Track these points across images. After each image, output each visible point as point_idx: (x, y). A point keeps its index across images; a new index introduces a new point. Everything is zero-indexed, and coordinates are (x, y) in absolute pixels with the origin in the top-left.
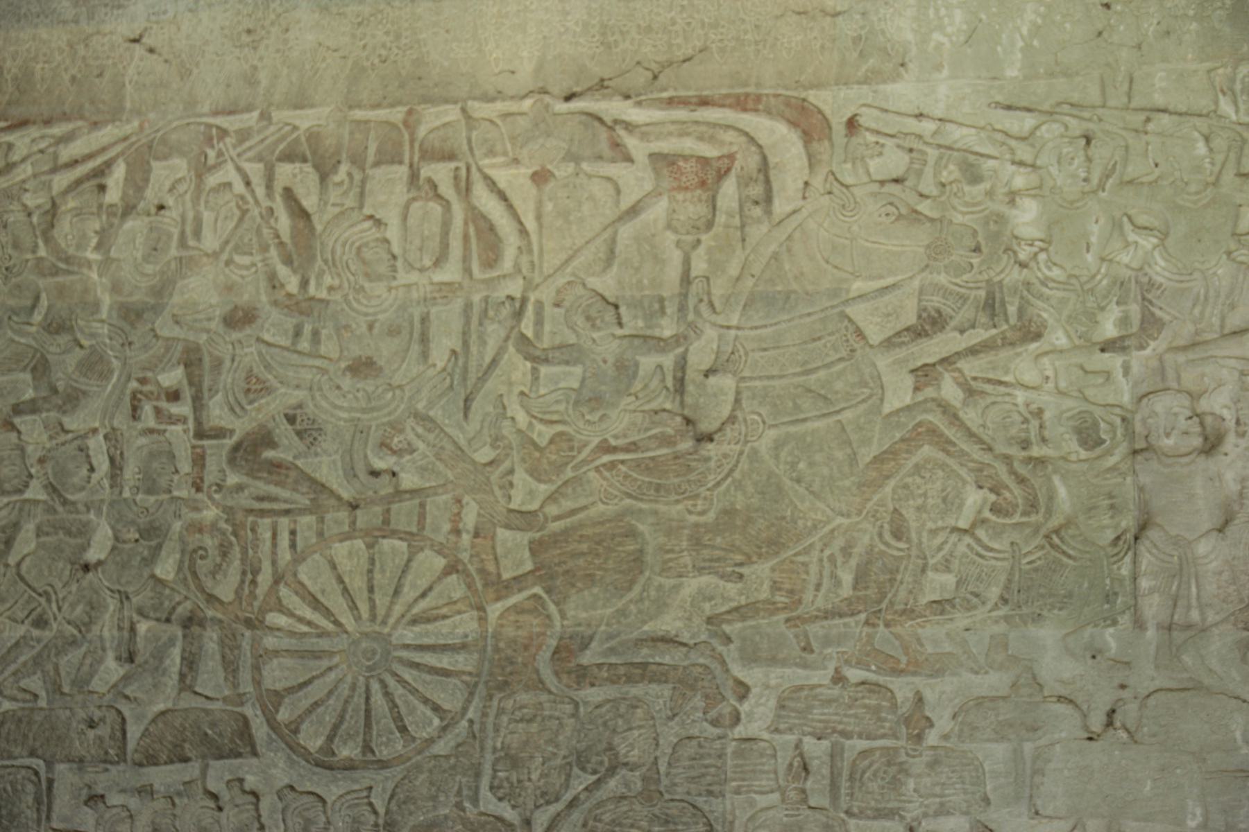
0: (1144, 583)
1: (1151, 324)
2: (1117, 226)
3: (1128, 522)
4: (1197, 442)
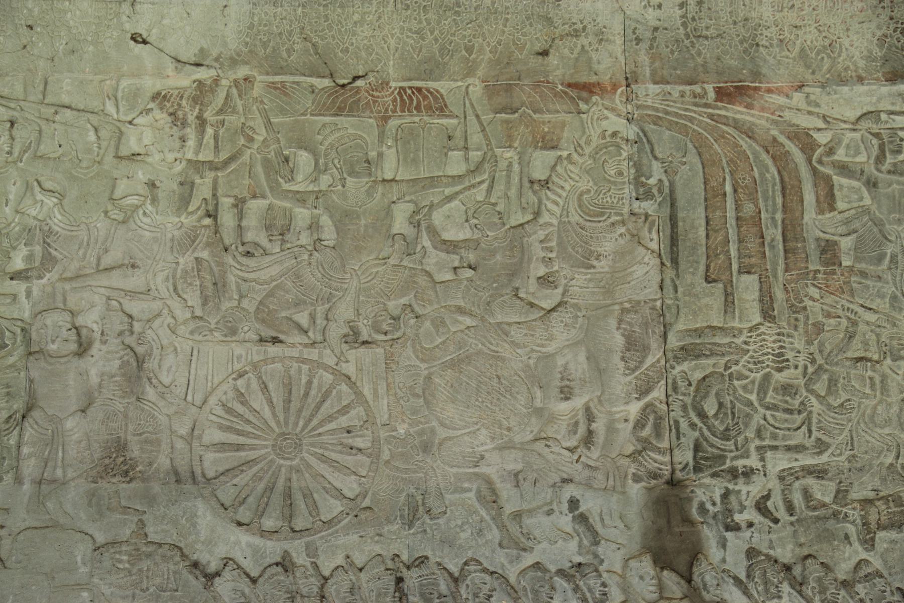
0: (25, 450)
1: (49, 261)
2: (28, 187)
3: (18, 405)
4: (73, 347)
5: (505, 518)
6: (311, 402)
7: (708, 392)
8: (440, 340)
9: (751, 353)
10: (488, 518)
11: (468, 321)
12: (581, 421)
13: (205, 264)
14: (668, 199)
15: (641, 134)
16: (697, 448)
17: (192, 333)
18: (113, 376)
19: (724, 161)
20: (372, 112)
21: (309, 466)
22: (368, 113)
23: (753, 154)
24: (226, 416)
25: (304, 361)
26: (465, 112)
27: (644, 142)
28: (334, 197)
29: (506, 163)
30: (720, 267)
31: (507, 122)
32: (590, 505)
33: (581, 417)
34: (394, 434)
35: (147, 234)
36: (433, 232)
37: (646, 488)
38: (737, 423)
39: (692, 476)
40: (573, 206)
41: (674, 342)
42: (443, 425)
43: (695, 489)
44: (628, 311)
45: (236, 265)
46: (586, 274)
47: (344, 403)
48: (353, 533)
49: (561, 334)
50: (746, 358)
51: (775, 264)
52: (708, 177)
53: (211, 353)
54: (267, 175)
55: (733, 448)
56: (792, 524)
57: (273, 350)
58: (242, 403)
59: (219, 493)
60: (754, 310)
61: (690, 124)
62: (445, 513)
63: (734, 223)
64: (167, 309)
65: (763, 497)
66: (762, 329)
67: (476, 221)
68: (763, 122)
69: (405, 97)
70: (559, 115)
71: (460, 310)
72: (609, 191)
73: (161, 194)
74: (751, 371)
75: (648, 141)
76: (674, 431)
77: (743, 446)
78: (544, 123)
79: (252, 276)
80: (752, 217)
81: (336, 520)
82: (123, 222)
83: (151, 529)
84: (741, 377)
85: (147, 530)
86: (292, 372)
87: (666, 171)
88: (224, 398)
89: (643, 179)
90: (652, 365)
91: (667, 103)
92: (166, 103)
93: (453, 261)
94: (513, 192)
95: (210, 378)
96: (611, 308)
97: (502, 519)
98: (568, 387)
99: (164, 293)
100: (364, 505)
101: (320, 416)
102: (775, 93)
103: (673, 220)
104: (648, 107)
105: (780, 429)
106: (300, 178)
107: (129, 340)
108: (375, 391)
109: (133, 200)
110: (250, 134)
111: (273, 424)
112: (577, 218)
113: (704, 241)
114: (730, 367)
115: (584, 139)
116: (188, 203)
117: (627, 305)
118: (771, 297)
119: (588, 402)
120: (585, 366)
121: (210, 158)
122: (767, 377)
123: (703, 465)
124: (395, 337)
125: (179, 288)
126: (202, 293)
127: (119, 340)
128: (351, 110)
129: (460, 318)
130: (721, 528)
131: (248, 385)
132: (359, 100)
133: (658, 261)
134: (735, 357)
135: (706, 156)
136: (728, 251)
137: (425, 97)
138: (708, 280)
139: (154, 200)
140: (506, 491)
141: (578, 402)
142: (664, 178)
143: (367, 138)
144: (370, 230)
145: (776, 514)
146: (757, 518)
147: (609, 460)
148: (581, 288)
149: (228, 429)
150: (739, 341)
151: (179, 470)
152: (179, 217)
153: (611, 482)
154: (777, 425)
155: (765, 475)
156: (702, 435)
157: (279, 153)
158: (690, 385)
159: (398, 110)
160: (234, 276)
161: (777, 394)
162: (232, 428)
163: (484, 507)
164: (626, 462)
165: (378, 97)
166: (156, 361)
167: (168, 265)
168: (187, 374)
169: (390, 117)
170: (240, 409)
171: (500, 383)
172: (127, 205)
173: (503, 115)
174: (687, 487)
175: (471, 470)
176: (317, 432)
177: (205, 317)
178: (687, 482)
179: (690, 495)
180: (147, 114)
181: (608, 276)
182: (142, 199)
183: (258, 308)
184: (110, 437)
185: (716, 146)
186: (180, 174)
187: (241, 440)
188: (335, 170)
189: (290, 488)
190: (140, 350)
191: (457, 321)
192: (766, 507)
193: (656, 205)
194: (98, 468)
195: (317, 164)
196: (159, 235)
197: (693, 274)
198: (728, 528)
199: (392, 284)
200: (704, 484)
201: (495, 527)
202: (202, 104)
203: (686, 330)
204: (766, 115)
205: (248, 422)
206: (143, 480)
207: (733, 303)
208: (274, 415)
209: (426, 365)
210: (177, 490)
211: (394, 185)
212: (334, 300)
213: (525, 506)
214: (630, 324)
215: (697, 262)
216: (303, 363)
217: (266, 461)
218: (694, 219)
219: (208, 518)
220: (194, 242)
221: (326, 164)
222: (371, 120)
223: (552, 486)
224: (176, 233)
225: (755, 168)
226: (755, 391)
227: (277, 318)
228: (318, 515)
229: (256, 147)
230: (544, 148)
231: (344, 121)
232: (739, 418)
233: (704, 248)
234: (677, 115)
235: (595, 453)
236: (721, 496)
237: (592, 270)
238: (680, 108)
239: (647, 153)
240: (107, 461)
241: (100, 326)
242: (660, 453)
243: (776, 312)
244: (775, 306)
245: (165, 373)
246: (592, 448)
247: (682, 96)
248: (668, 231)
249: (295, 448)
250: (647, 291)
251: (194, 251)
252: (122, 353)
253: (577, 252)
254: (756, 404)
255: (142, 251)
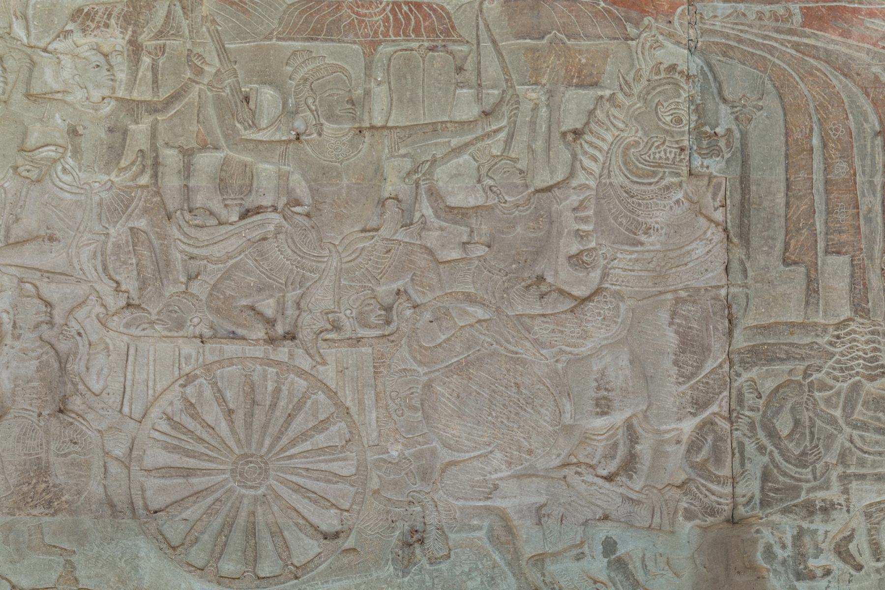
5: (523, 563)
6: (279, 414)
7: (782, 407)
8: (444, 337)
9: (837, 357)
10: (502, 563)
11: (480, 313)
12: (621, 442)
13: (142, 237)
14: (739, 154)
15: (706, 69)
16: (766, 476)
17: (128, 325)
18: (29, 381)
19: (812, 106)
20: (356, 35)
21: (278, 497)
22: (351, 36)
23: (849, 97)
24: (173, 433)
25: (271, 363)
26: (478, 36)
27: (712, 81)
28: (309, 149)
29: (530, 106)
30: (802, 245)
31: (534, 50)
32: (630, 547)
33: (621, 436)
34: (384, 456)
35: (67, 195)
36: (434, 194)
37: (700, 527)
38: (817, 446)
39: (758, 512)
40: (617, 163)
41: (740, 341)
42: (446, 445)
43: (761, 528)
44: (684, 301)
45: (182, 237)
46: (632, 252)
47: (322, 417)
48: (334, 581)
49: (598, 330)
50: (831, 363)
51: (871, 241)
52: (790, 126)
53: (152, 352)
54: (221, 119)
55: (810, 476)
56: (878, 571)
57: (232, 349)
58: (192, 416)
59: (166, 529)
60: (844, 301)
61: (769, 57)
62: (449, 557)
63: (821, 187)
64: (95, 294)
65: (845, 538)
66: (853, 326)
67: (491, 182)
68: (863, 55)
69: (400, 16)
70: (601, 41)
71: (470, 299)
72: (663, 143)
73: (85, 144)
74: (836, 379)
75: (715, 78)
76: (737, 455)
77: (823, 475)
78: (580, 52)
79: (203, 252)
80: (846, 181)
81: (312, 565)
82: (38, 181)
83: (83, 573)
84: (823, 387)
85: (77, 574)
86: (256, 377)
87: (737, 119)
88: (169, 410)
89: (707, 129)
90: (711, 372)
91: (741, 27)
92: (89, 23)
93: (461, 234)
94: (539, 145)
95: (151, 384)
96: (663, 297)
97: (519, 565)
98: (605, 398)
99: (92, 275)
100: (347, 546)
101: (290, 434)
102: (879, 17)
103: (744, 181)
104: (714, 32)
105: (869, 453)
106: (264, 123)
107: (47, 333)
108: (361, 403)
109: (49, 152)
110: (199, 64)
111: (232, 443)
112: (621, 179)
113: (782, 211)
114: (811, 375)
115: (632, 73)
116: (120, 155)
117: (683, 294)
118: (864, 285)
119: (630, 417)
120: (628, 372)
121: (148, 97)
122: (856, 388)
123: (772, 498)
124: (387, 333)
125: (110, 267)
126: (138, 274)
127: (35, 335)
128: (329, 32)
129: (470, 309)
130: (791, 576)
131: (200, 394)
132: (340, 19)
133: (723, 235)
134: (818, 362)
135: (789, 99)
136: (813, 225)
137: (426, 17)
138: (786, 262)
139: (77, 152)
140: (525, 528)
141: (618, 418)
142: (734, 127)
143: (351, 71)
144: (355, 192)
145: (859, 559)
146: (836, 564)
147: (655, 491)
148: (625, 270)
149: (176, 449)
150: (823, 341)
151: (116, 500)
152: (109, 175)
153: (657, 519)
154: (865, 448)
155: (848, 511)
156: (772, 460)
157: (236, 89)
158: (760, 397)
159: (391, 33)
160: (181, 252)
161: (868, 409)
162: (180, 448)
163: (498, 549)
164: (676, 493)
165: (365, 15)
166: (83, 363)
167: (96, 237)
168: (122, 379)
169: (380, 43)
170: (190, 424)
171: (519, 392)
172: (42, 159)
173: (528, 41)
174: (751, 525)
175: (481, 504)
176: (287, 454)
177: (143, 306)
178: (752, 520)
179: (755, 535)
180: (65, 38)
181: (660, 255)
182: (61, 150)
183: (211, 294)
184: (27, 458)
185: (802, 86)
186: (108, 117)
187: (191, 463)
188: (309, 113)
189: (254, 524)
190: (63, 346)
191: (466, 313)
192: (848, 550)
193: (723, 164)
194: (15, 497)
195: (285, 104)
196: (83, 198)
197: (768, 254)
198: (799, 576)
199: (382, 264)
200: (773, 522)
201: (511, 575)
202: (136, 25)
203: (756, 327)
204: (866, 45)
205: (201, 440)
206: (72, 512)
207: (817, 292)
208: (233, 430)
209: (426, 370)
210: (113, 526)
211: (385, 132)
212: (308, 285)
213: (549, 549)
214: (686, 318)
215: (773, 239)
216: (269, 365)
217: (224, 490)
218: (770, 179)
219: (153, 561)
220: (127, 207)
221: (297, 105)
222: (355, 47)
223: (583, 524)
224: (105, 195)
225: (850, 117)
226: (841, 405)
227: (236, 307)
228: (290, 556)
229: (206, 81)
230: (580, 86)
231: (320, 47)
232: (819, 439)
233: (783, 220)
234: (752, 43)
235: (638, 483)
236: (793, 537)
237: (639, 248)
238: (756, 35)
239: (712, 93)
240: (25, 488)
241: (11, 316)
242: (719, 483)
243: (870, 304)
244: (870, 296)
245: (95, 377)
246: (635, 476)
247: (760, 19)
248: (737, 197)
249: (260, 474)
250: (710, 275)
251: (127, 220)
252: (40, 351)
253: (621, 224)
254: (841, 422)
255: (62, 220)
